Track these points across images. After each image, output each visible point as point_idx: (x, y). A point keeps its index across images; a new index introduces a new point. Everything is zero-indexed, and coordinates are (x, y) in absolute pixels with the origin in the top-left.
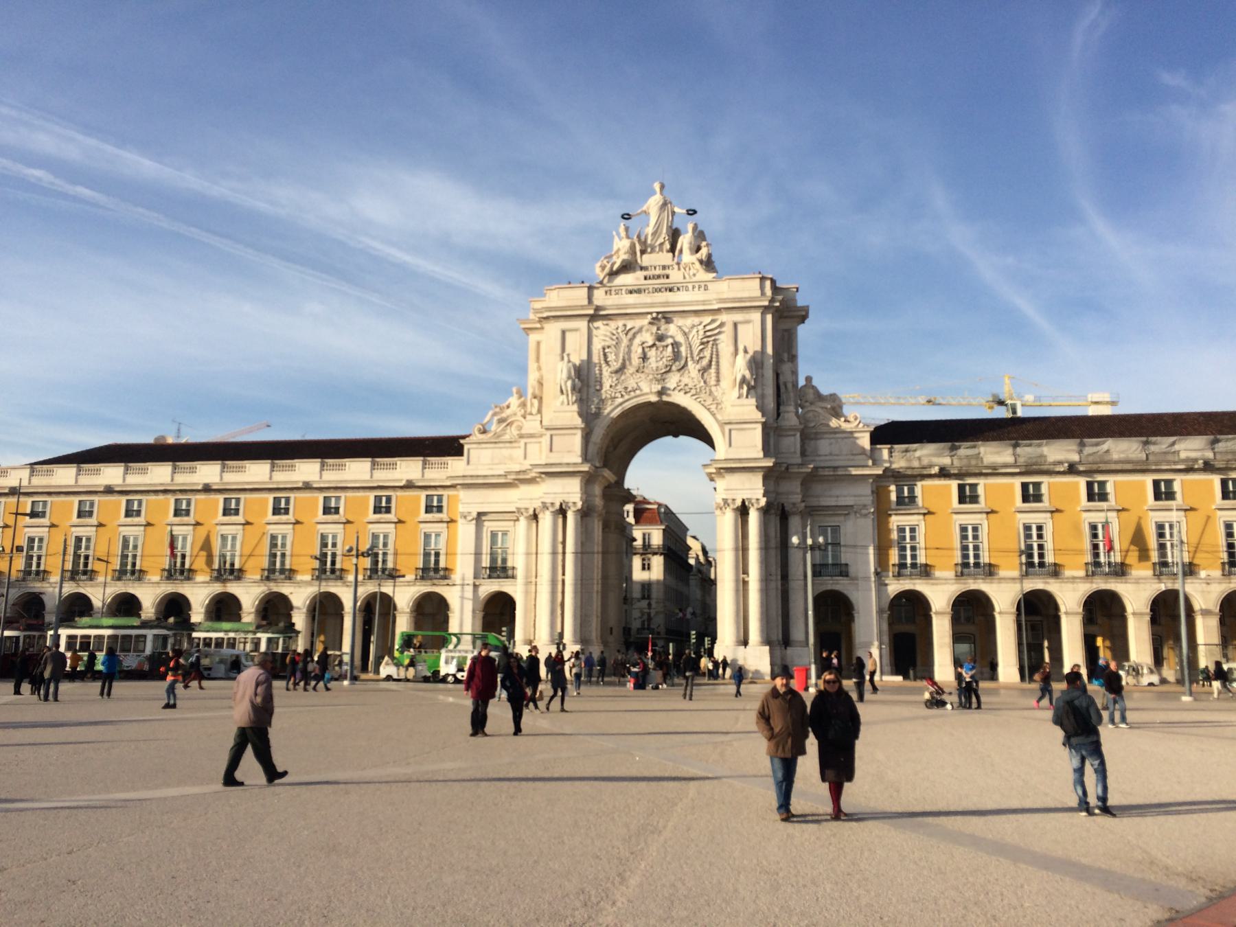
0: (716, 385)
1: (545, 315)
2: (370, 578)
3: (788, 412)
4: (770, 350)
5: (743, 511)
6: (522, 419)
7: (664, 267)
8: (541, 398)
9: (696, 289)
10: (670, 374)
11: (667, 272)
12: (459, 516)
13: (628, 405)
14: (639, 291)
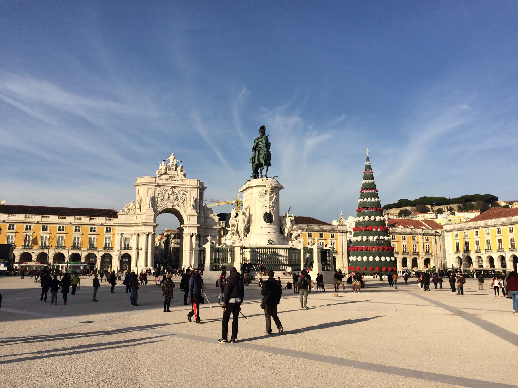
1: (144, 184)
2: (89, 249)
3: (201, 212)
4: (198, 198)
7: (174, 175)
11: (175, 176)
12: (116, 233)
13: (164, 208)
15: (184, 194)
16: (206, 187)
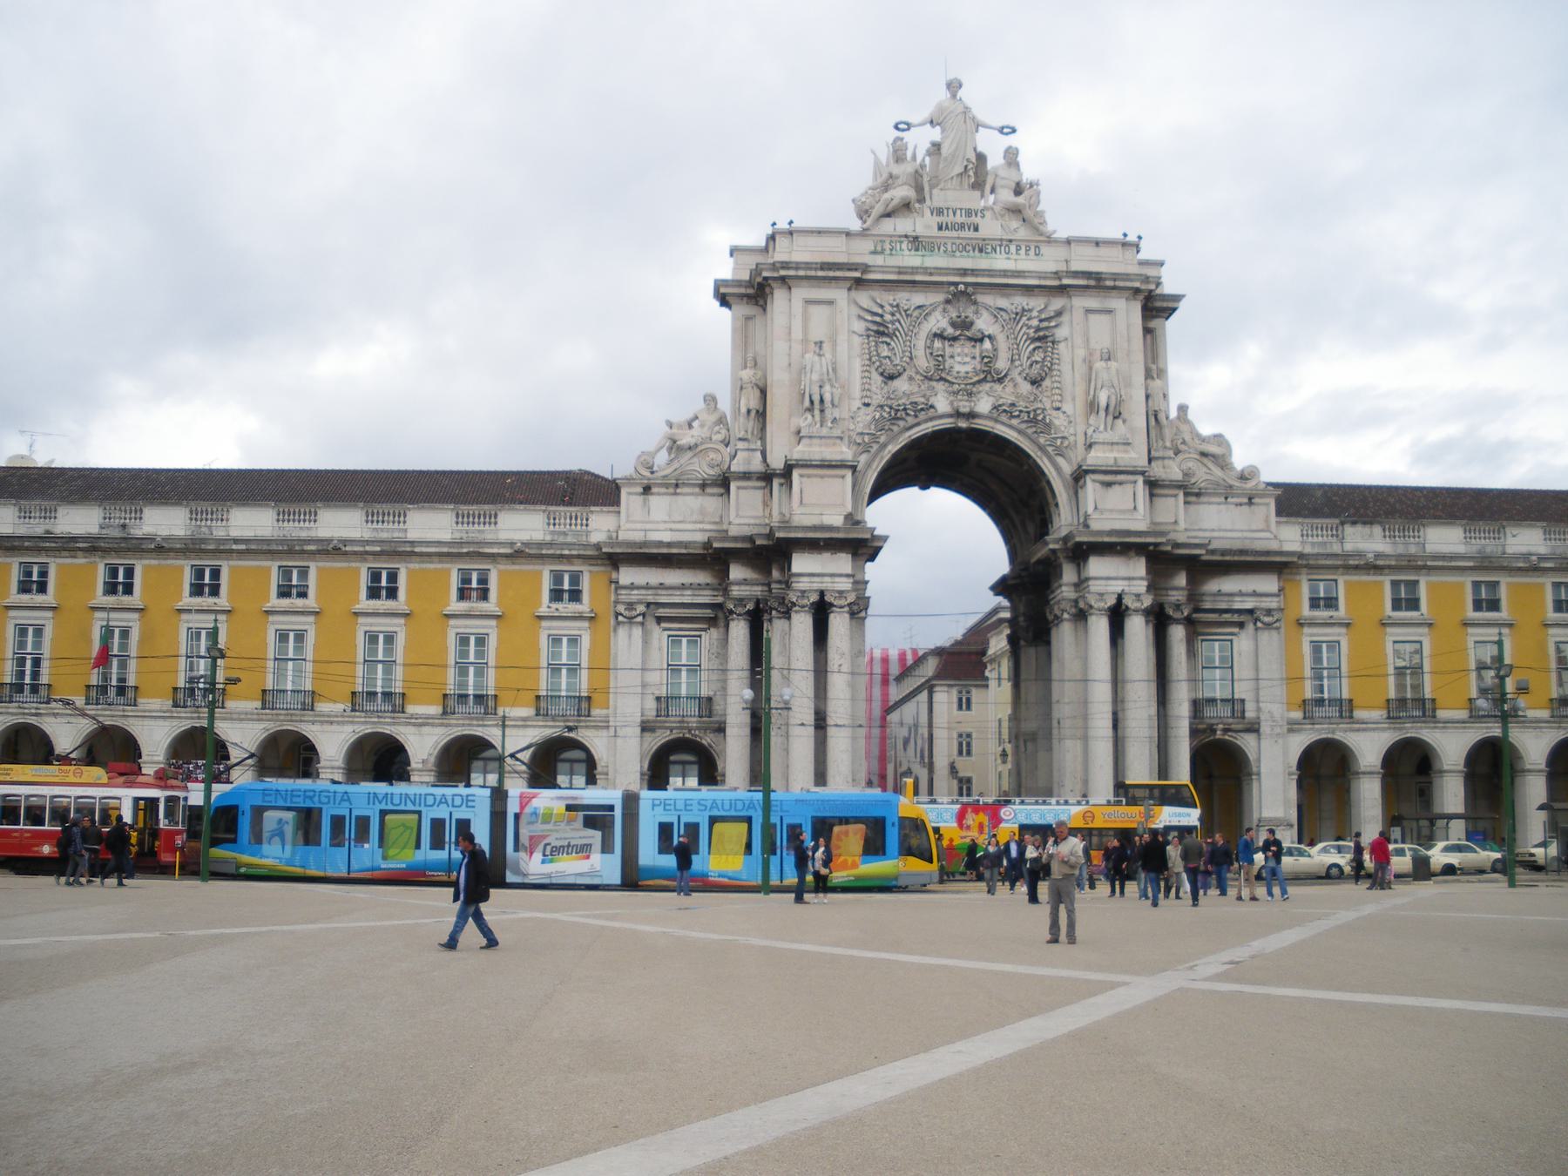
0: (1058, 409)
5: (1117, 616)
6: (721, 447)
7: (969, 213)
8: (762, 415)
9: (1023, 251)
10: (987, 386)
11: (974, 219)
13: (916, 433)
16: (1184, 296)
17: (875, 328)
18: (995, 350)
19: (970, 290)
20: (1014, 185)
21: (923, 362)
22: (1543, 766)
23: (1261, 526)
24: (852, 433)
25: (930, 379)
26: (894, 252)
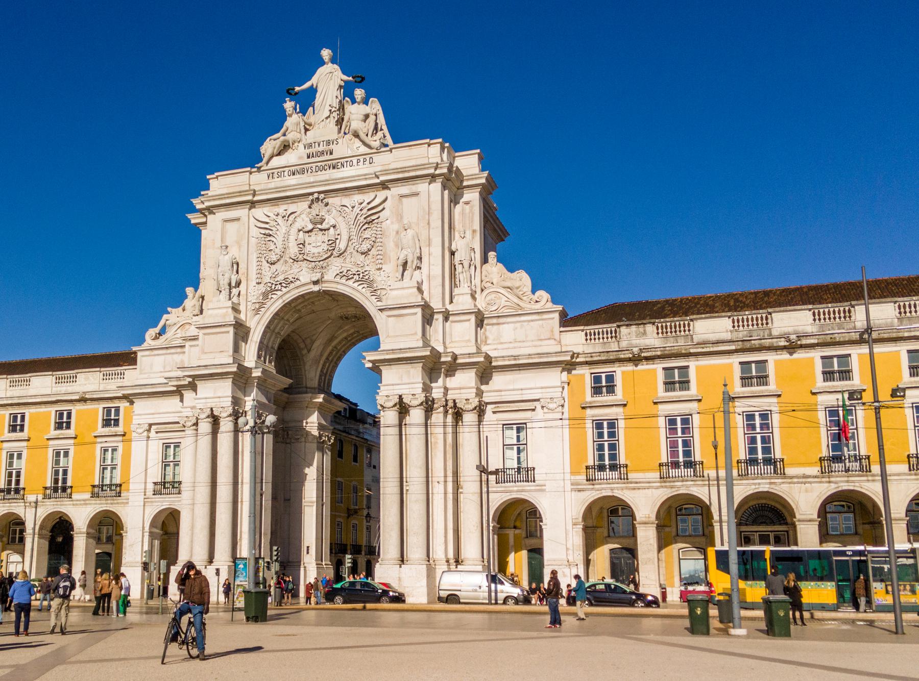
0: (380, 269)
13: (289, 297)
14: (302, 172)
15: (368, 219)
17: (263, 231)
18: (338, 235)
19: (322, 196)
20: (362, 117)
21: (293, 250)
22: (815, 516)
23: (549, 337)
24: (248, 303)
25: (297, 261)
26: (280, 179)
